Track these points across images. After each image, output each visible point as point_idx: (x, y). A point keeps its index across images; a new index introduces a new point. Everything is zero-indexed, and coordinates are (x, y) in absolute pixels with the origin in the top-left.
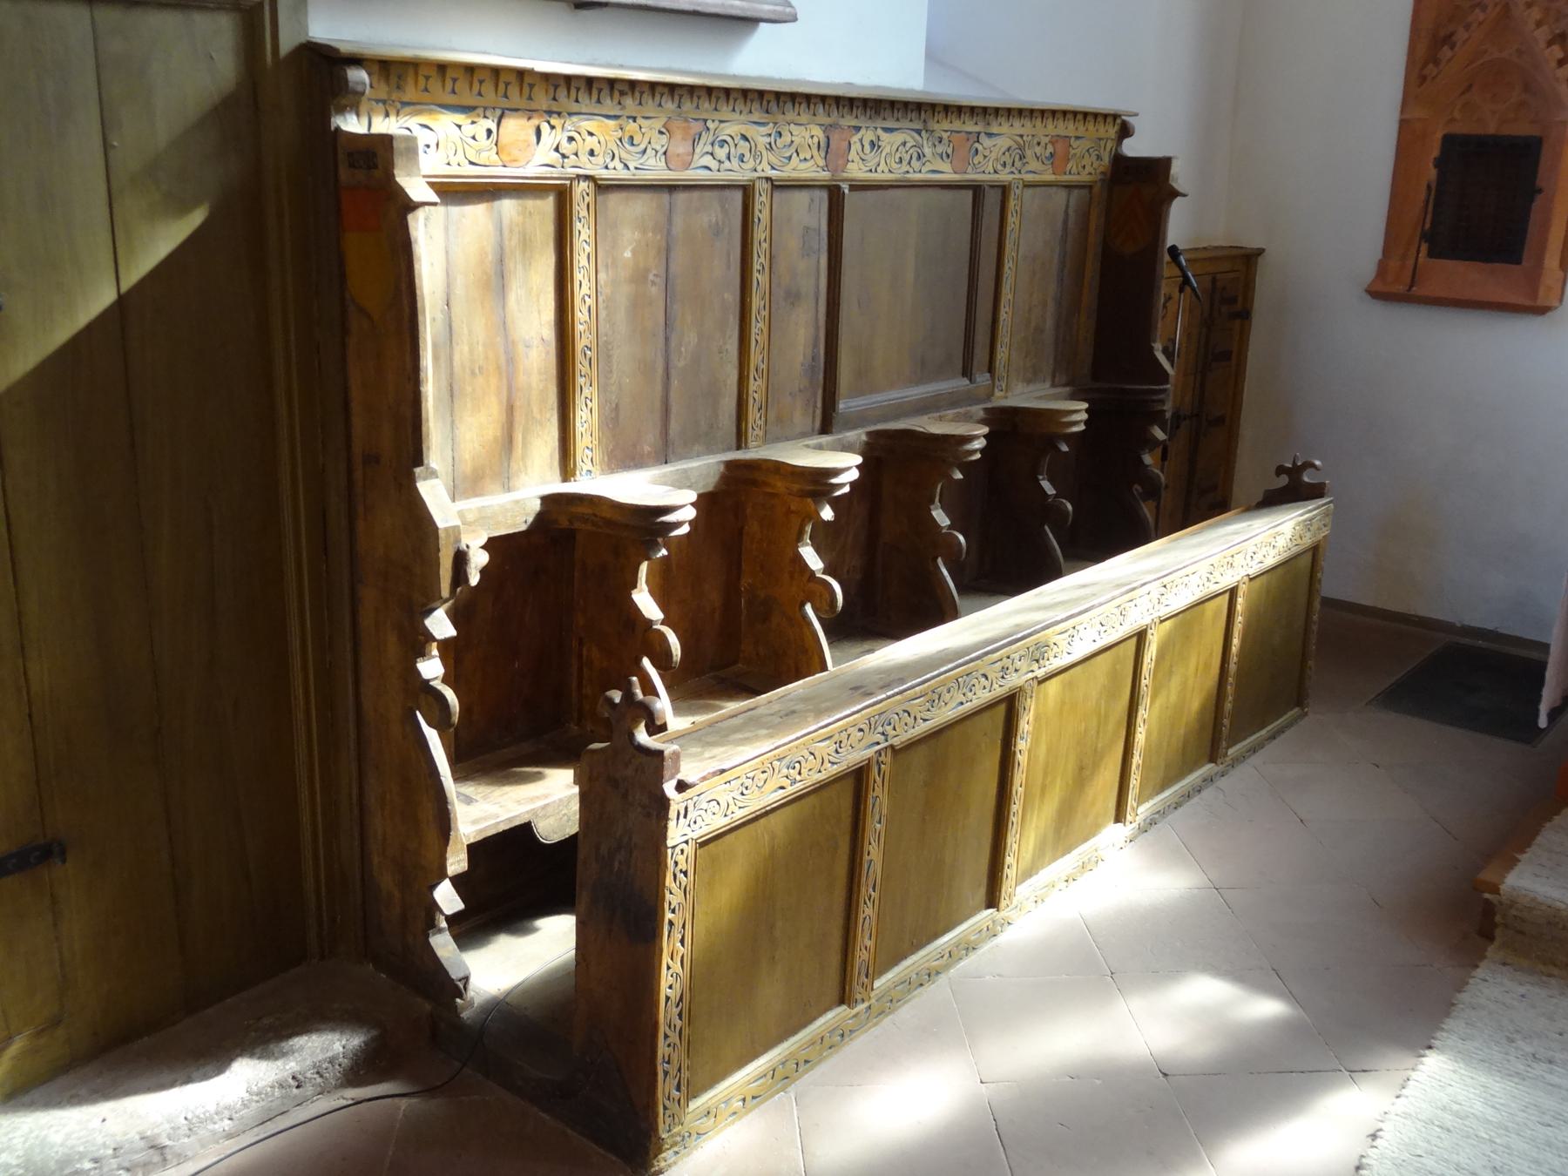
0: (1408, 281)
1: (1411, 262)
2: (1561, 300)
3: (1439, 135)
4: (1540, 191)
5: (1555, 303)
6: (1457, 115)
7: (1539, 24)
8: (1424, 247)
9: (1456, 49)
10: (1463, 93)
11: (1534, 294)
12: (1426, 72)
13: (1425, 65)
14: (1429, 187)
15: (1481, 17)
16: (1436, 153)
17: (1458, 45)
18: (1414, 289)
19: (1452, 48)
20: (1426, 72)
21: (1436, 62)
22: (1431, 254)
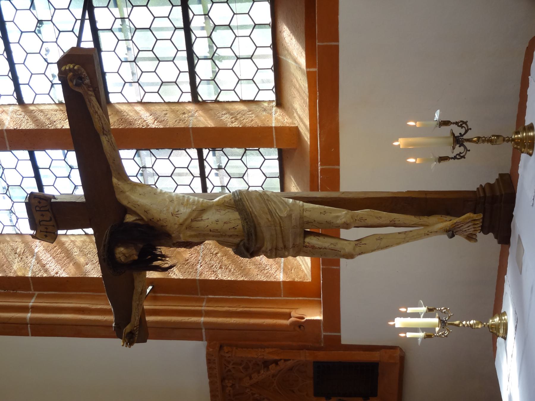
5: (398, 353)
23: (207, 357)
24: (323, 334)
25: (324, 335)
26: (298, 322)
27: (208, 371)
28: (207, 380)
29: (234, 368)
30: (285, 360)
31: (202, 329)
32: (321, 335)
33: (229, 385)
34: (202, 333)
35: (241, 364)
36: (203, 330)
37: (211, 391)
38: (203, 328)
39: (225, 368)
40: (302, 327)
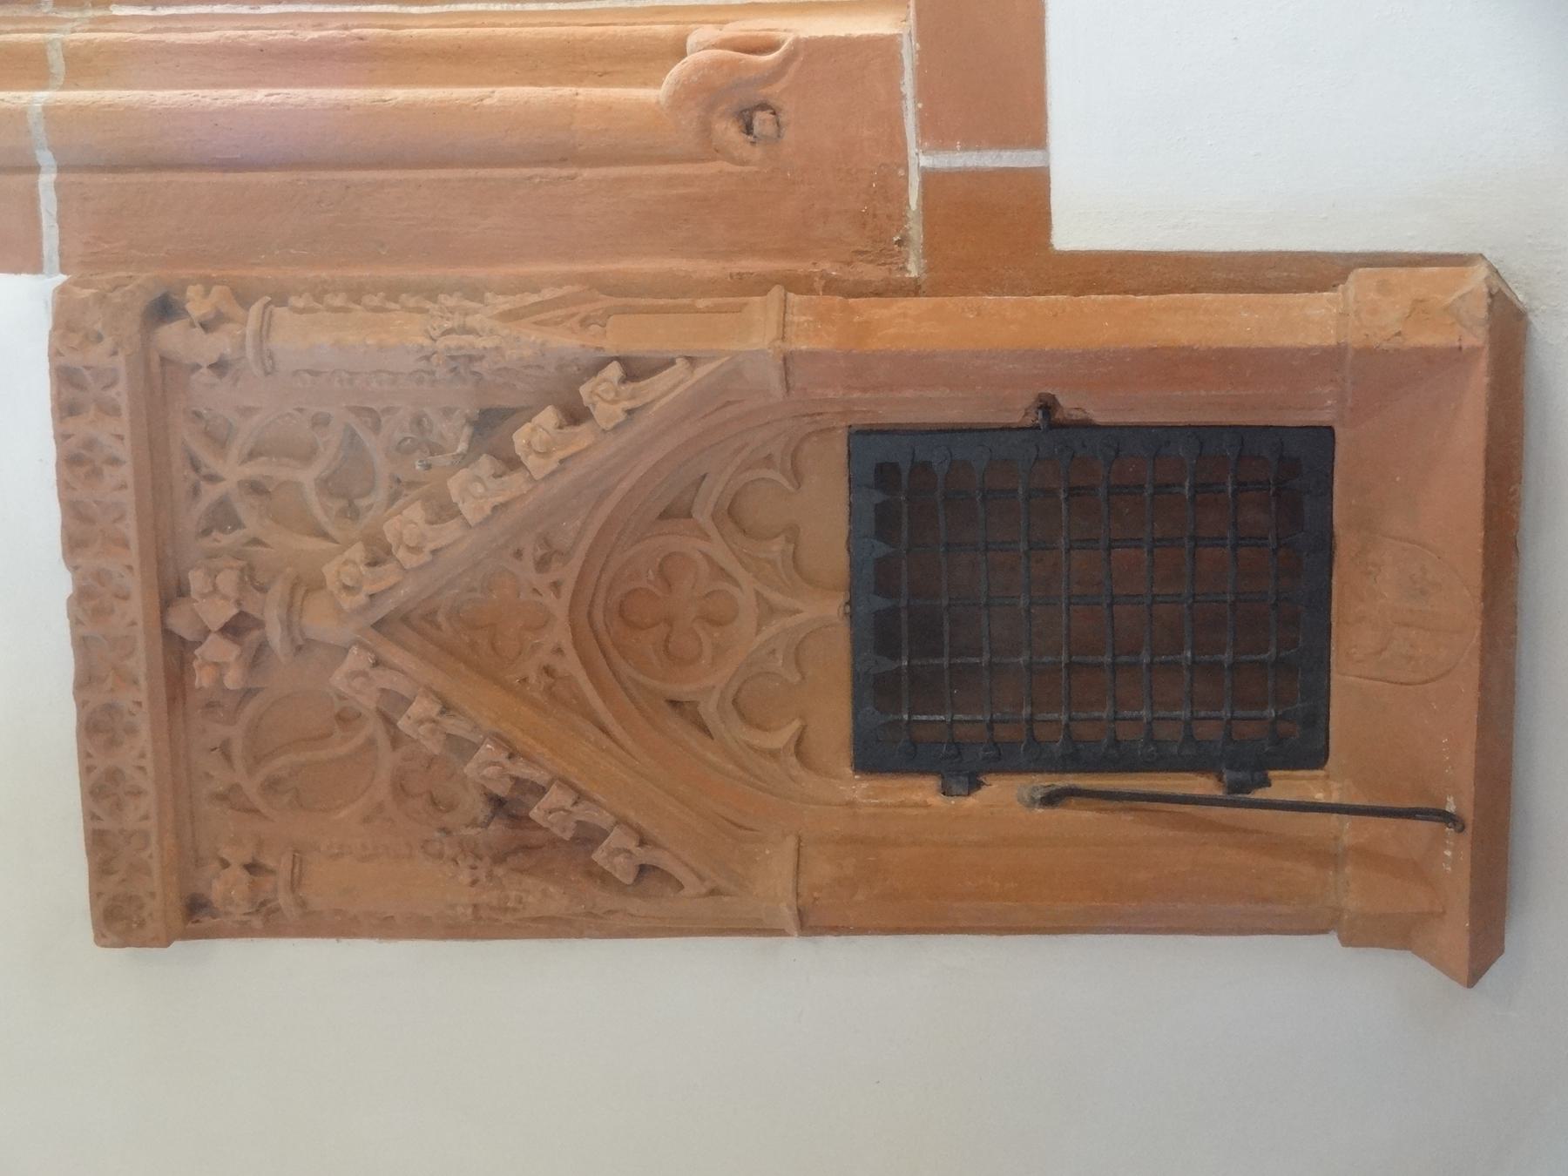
0: (1422, 828)
1: (1348, 830)
2: (1460, 260)
3: (860, 789)
4: (1047, 406)
5: (1477, 277)
6: (781, 738)
7: (444, 511)
8: (1285, 785)
9: (538, 776)
10: (704, 729)
11: (1454, 359)
12: (622, 870)
13: (604, 878)
14: (1052, 799)
15: (422, 707)
16: (923, 792)
17: (522, 770)
18: (1451, 807)
19: (541, 791)
20: (622, 870)
21: (588, 837)
22: (1313, 756)
23: (54, 354)
24: (921, 160)
25: (929, 177)
26: (734, 65)
27: (64, 486)
28: (60, 584)
29: (256, 488)
30: (635, 370)
31: (35, 169)
32: (906, 178)
33: (220, 612)
34: (33, 199)
35: (307, 456)
36: (47, 180)
37: (85, 681)
38: (45, 158)
39: (195, 491)
40: (762, 120)
